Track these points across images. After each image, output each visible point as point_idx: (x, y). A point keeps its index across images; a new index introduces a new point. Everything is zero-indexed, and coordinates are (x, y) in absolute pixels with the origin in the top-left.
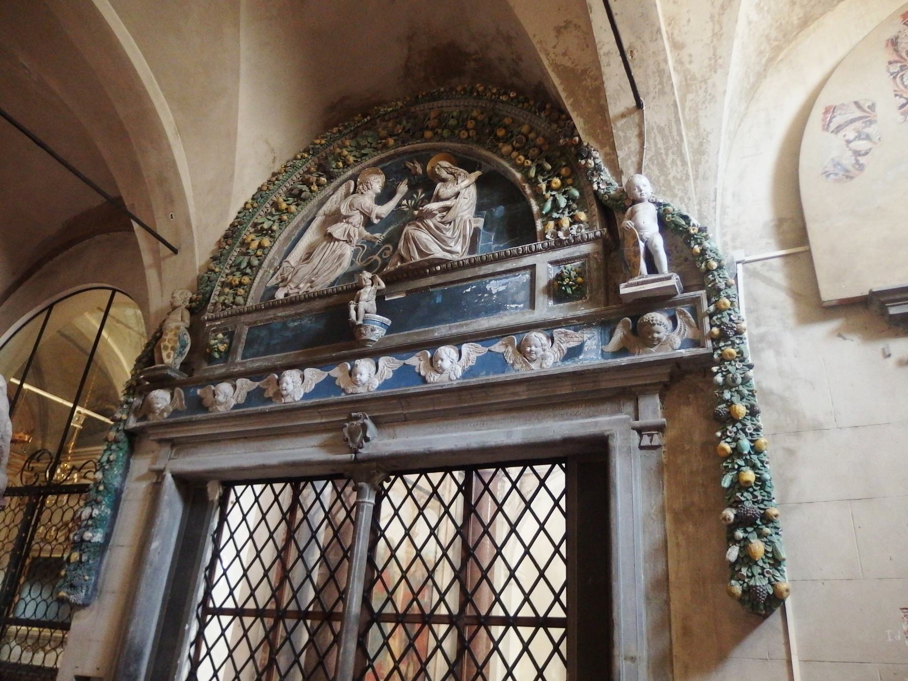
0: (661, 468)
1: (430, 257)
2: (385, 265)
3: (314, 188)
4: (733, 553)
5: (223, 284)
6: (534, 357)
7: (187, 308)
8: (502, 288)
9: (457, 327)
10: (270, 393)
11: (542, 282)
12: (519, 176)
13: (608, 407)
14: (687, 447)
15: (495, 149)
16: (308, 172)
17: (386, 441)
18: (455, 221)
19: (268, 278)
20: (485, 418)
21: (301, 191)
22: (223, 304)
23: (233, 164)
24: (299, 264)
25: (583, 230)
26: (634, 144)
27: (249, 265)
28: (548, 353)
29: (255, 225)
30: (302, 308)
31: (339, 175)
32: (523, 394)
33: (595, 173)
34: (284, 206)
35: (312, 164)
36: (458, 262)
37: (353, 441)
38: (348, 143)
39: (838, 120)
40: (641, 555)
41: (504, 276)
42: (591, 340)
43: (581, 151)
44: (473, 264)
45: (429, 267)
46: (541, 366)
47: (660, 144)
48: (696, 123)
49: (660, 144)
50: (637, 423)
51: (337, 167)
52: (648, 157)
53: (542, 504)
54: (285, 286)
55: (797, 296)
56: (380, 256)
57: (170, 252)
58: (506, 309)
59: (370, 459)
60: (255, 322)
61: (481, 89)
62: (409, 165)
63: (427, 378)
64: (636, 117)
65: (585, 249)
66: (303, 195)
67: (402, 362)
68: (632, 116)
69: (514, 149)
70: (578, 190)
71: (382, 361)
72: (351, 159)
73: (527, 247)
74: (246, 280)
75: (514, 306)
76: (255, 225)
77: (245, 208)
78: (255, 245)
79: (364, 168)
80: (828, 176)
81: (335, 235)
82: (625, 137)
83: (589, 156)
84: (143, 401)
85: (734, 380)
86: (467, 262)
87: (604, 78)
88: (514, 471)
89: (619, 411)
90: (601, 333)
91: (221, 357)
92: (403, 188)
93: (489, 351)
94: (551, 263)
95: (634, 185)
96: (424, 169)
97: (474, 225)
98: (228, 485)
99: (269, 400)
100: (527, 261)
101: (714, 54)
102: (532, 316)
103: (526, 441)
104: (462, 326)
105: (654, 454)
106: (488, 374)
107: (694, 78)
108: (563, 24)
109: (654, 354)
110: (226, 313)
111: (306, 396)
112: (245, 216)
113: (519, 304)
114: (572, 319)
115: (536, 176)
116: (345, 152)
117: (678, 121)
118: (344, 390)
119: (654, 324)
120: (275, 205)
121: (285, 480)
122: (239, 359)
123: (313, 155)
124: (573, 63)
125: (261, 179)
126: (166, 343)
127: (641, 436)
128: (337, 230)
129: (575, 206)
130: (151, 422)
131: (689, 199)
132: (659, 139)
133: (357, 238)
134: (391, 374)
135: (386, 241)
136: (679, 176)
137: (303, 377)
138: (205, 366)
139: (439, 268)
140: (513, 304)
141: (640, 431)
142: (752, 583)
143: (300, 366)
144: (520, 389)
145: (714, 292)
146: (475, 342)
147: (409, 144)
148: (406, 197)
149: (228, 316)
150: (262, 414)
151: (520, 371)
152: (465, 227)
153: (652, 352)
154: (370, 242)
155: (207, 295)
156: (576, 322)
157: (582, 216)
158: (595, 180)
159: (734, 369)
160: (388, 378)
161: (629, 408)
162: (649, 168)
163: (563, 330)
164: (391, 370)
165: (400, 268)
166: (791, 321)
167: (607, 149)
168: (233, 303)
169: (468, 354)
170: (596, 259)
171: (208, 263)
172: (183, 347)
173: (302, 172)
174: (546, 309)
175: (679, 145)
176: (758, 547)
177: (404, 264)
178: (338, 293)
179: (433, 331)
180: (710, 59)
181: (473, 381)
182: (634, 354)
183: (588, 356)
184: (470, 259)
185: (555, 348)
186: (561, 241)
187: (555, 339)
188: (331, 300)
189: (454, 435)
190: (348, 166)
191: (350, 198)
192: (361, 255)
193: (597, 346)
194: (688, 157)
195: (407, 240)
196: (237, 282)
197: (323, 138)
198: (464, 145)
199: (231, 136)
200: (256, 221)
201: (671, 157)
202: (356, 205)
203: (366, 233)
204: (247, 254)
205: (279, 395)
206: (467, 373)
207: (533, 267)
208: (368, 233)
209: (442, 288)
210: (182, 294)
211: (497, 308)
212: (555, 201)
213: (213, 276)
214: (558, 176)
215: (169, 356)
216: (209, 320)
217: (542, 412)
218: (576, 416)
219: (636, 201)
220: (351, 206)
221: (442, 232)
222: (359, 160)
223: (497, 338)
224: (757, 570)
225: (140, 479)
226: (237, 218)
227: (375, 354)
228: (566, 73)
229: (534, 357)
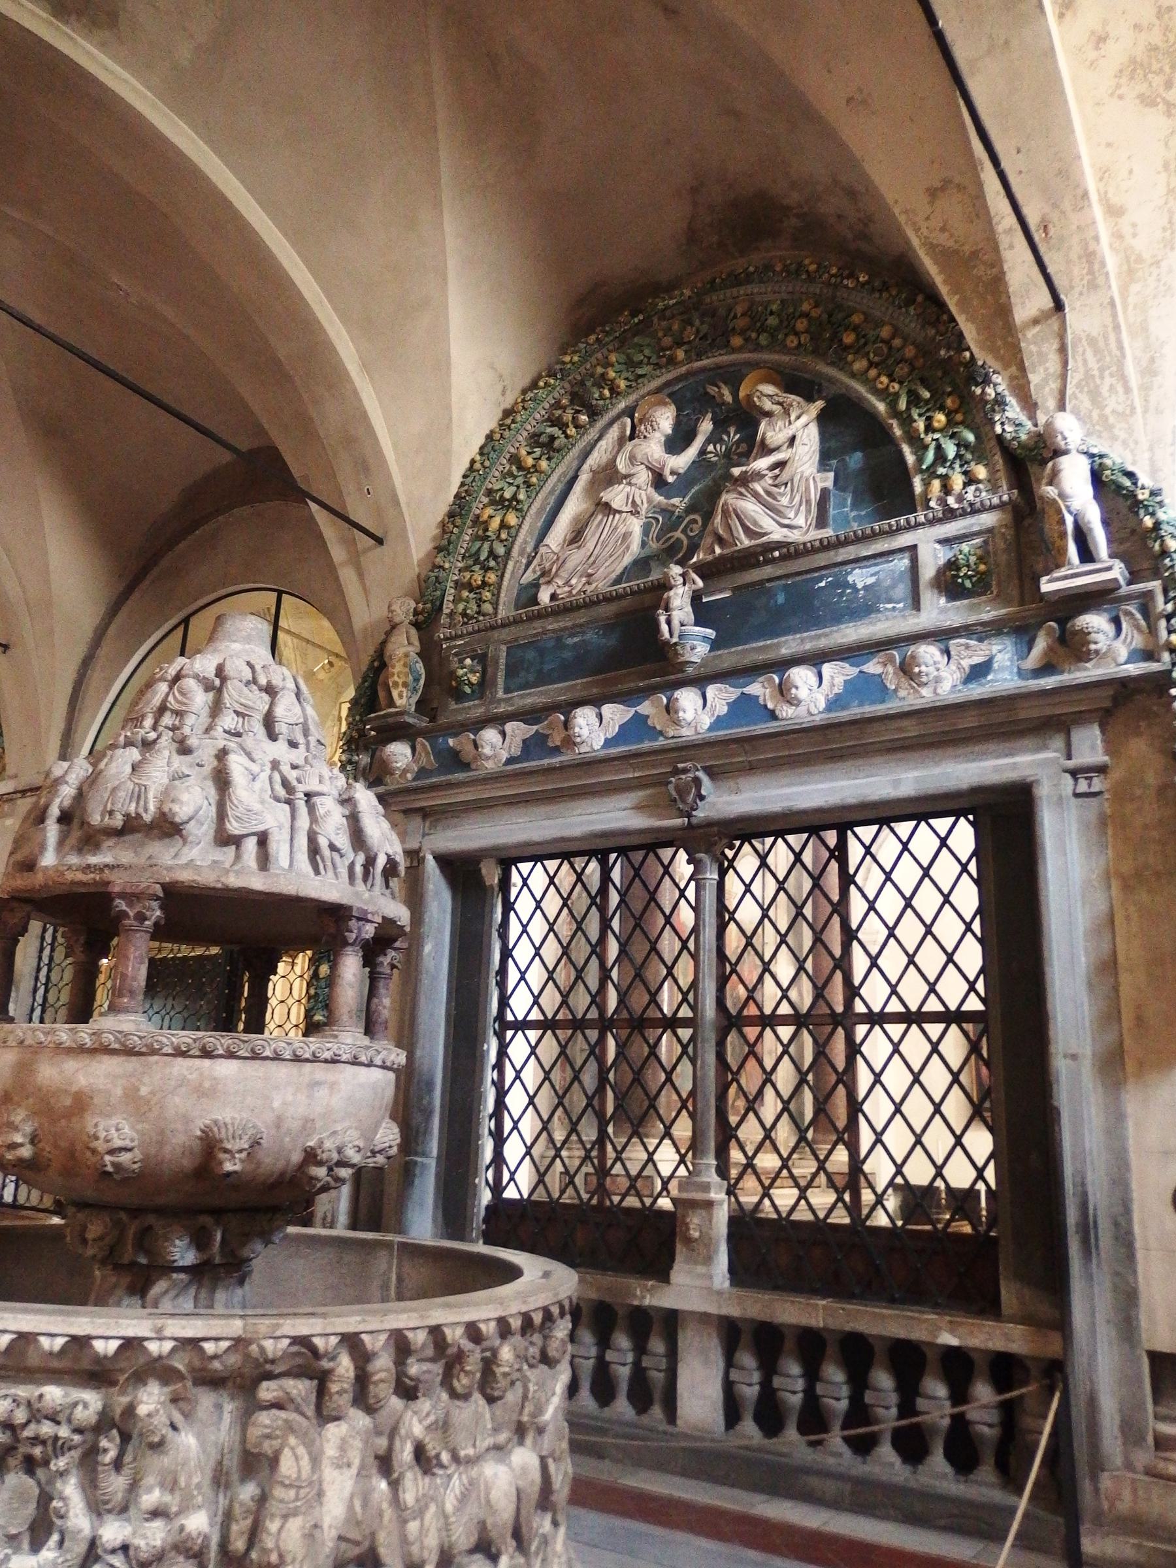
0: (1103, 821)
1: (764, 539)
2: (693, 549)
3: (572, 431)
5: (458, 585)
6: (924, 679)
7: (411, 623)
8: (871, 580)
9: (812, 638)
10: (556, 740)
11: (928, 572)
12: (881, 407)
13: (1027, 742)
14: (1138, 792)
15: (841, 363)
16: (557, 405)
17: (726, 798)
18: (792, 480)
19: (521, 572)
20: (860, 762)
21: (552, 438)
22: (464, 614)
23: (448, 407)
25: (984, 494)
26: (1053, 363)
27: (492, 554)
28: (943, 674)
29: (489, 492)
30: (581, 617)
32: (912, 729)
33: (996, 408)
34: (530, 461)
35: (559, 390)
36: (804, 544)
37: (684, 801)
38: (613, 358)
40: (1080, 931)
41: (872, 561)
42: (1002, 652)
43: (975, 375)
44: (826, 546)
45: (763, 553)
46: (935, 692)
48: (1144, 328)
50: (1071, 764)
51: (602, 397)
52: (1074, 382)
53: (945, 870)
54: (549, 583)
56: (684, 531)
58: (878, 611)
59: (709, 824)
60: (516, 640)
61: (813, 267)
62: (712, 390)
63: (777, 712)
64: (1054, 323)
65: (987, 520)
66: (556, 444)
67: (741, 690)
68: (1049, 322)
69: (871, 364)
70: (972, 430)
71: (711, 690)
72: (622, 384)
73: (902, 520)
74: (492, 577)
75: (890, 606)
77: (471, 468)
78: (495, 524)
79: (643, 397)
81: (615, 505)
82: (1040, 353)
83: (987, 381)
84: (372, 757)
86: (817, 544)
87: (1006, 267)
88: (904, 828)
89: (1045, 748)
90: (1016, 644)
91: (473, 691)
92: (706, 426)
93: (861, 672)
94: (940, 542)
95: (1055, 431)
96: (735, 394)
97: (821, 485)
98: (507, 860)
99: (556, 750)
101: (1170, 222)
102: (916, 620)
103: (922, 793)
104: (819, 637)
105: (1094, 802)
106: (861, 704)
107: (1140, 259)
108: (939, 185)
109: (1090, 672)
110: (470, 629)
111: (608, 743)
112: (473, 481)
113: (898, 603)
114: (974, 625)
115: (908, 409)
116: (612, 374)
117: (1117, 328)
118: (661, 733)
119: (1089, 633)
120: (515, 459)
121: (590, 854)
122: (500, 694)
123: (562, 379)
124: (956, 242)
125: (490, 423)
126: (396, 678)
127: (1076, 780)
128: (616, 496)
129: (969, 456)
130: (392, 787)
131: (1136, 443)
132: (1089, 354)
133: (646, 505)
134: (725, 709)
135: (690, 509)
136: (1120, 409)
137: (600, 717)
138: (453, 706)
139: (777, 554)
140: (889, 603)
141: (1074, 773)
143: (596, 702)
144: (905, 723)
146: (842, 660)
147: (708, 358)
148: (711, 439)
149: (474, 632)
150: (550, 770)
151: (907, 698)
152: (807, 489)
153: (1086, 669)
154: (665, 511)
155: (438, 603)
156: (980, 629)
157: (981, 472)
158: (997, 418)
160: (722, 714)
161: (1058, 742)
162: (1076, 398)
163: (962, 641)
164: (724, 702)
165: (721, 556)
167: (1013, 370)
168: (478, 613)
169: (832, 677)
170: (1003, 534)
171: (428, 555)
172: (417, 680)
173: (547, 406)
175: (1120, 364)
177: (726, 551)
178: (633, 593)
179: (778, 646)
180: (1164, 229)
181: (843, 715)
182: (1062, 672)
183: (1000, 676)
184: (821, 540)
185: (953, 667)
186: (952, 510)
187: (952, 653)
188: (624, 603)
189: (820, 786)
190: (618, 394)
191: (629, 446)
192: (655, 530)
193: (1011, 660)
194: (1134, 380)
195: (726, 513)
197: (574, 352)
198: (794, 358)
199: (442, 366)
200: (490, 486)
201: (1108, 381)
202: (639, 457)
203: (658, 498)
204: (485, 538)
205: (570, 742)
206: (834, 703)
207: (913, 548)
208: (661, 498)
209: (783, 582)
210: (403, 604)
211: (865, 608)
212: (939, 448)
213: (442, 574)
214: (942, 408)
215: (401, 696)
216: (446, 639)
217: (940, 752)
218: (984, 755)
219: (1058, 453)
220: (632, 459)
221: (775, 499)
222: (634, 384)
223: (872, 653)
226: (462, 484)
227: (700, 681)
228: (945, 256)
229: (924, 679)
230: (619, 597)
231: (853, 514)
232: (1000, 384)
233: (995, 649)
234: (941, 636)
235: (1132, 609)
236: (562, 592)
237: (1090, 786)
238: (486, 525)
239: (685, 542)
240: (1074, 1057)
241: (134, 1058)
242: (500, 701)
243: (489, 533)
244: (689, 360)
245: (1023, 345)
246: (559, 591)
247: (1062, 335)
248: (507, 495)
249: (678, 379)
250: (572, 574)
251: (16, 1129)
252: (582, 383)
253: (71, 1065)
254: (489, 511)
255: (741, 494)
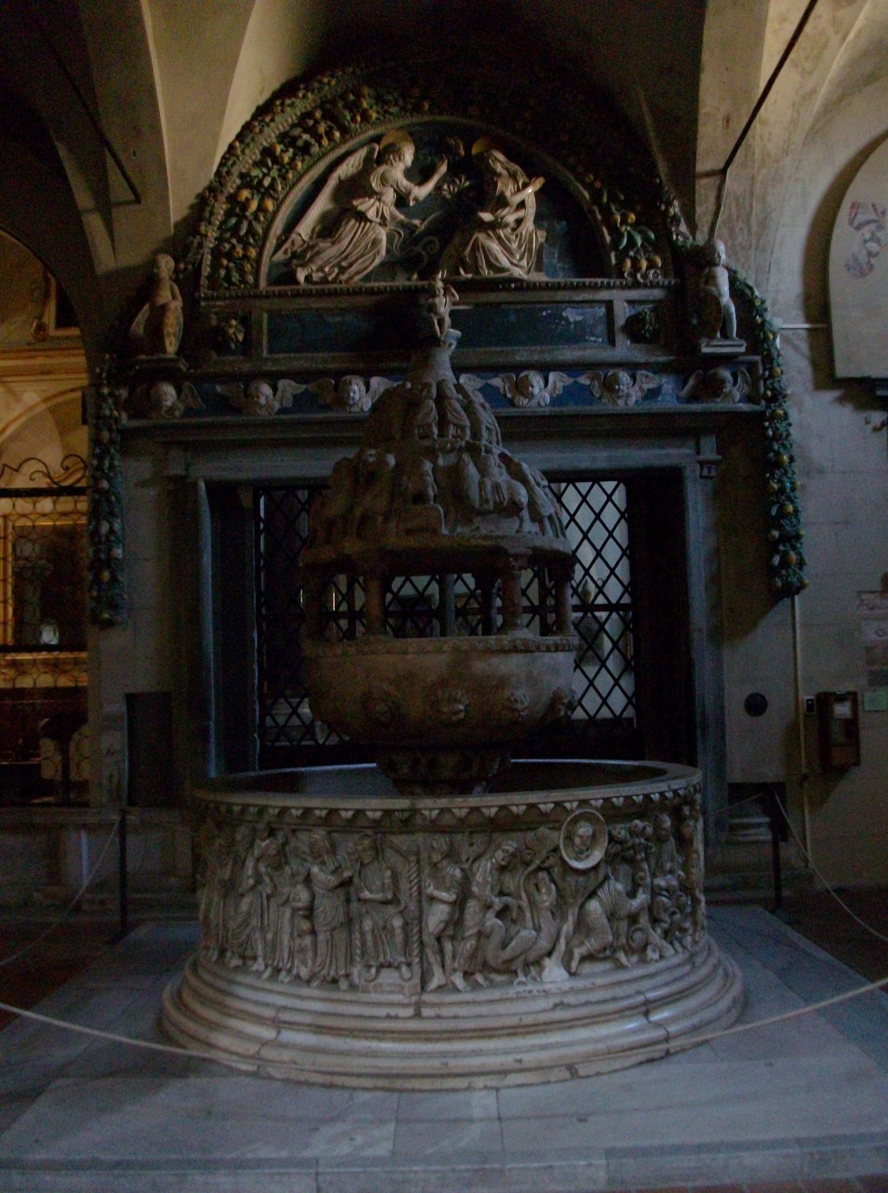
3: (325, 142)
4: (776, 560)
6: (621, 394)
8: (579, 318)
11: (620, 320)
16: (309, 115)
24: (311, 238)
26: (711, 204)
28: (632, 392)
29: (242, 176)
30: (344, 302)
31: (357, 134)
36: (534, 284)
38: (366, 91)
39: (861, 218)
42: (668, 384)
44: (547, 287)
46: (626, 404)
47: (734, 210)
48: (764, 199)
49: (734, 210)
50: (701, 457)
53: (611, 516)
55: (815, 365)
57: (132, 197)
58: (586, 341)
63: (516, 401)
67: (484, 382)
72: (374, 115)
75: (593, 339)
76: (242, 176)
78: (254, 205)
80: (849, 269)
83: (669, 204)
85: (781, 436)
87: (699, 136)
88: (584, 487)
92: (443, 169)
93: (576, 382)
96: (468, 148)
99: (327, 407)
100: (604, 295)
101: (789, 138)
105: (709, 481)
107: (769, 155)
109: (718, 405)
113: (598, 337)
117: (752, 193)
122: (265, 354)
128: (369, 207)
132: (733, 205)
135: (428, 232)
138: (214, 356)
139: (513, 285)
141: (702, 464)
142: (789, 580)
143: (366, 376)
145: (769, 359)
146: (561, 371)
148: (447, 178)
151: (605, 406)
157: (659, 262)
158: (673, 229)
159: (781, 426)
166: (810, 386)
169: (555, 383)
171: (185, 220)
173: (299, 113)
174: (625, 350)
176: (793, 556)
180: (785, 142)
184: (547, 283)
190: (368, 122)
193: (673, 390)
194: (754, 229)
196: (241, 255)
201: (740, 224)
202: (391, 181)
214: (633, 210)
215: (171, 344)
216: (206, 299)
224: (791, 572)
225: (142, 484)
226: (222, 165)
230: (371, 292)
231: (559, 265)
232: (675, 209)
233: (664, 380)
234: (632, 367)
235: (743, 369)
236: (316, 277)
237: (709, 472)
238: (245, 206)
239: (426, 258)
240: (700, 630)
241: (528, 654)
242: (267, 359)
243: (248, 214)
244: (431, 111)
245: (697, 187)
246: (314, 275)
247: (720, 189)
248: (267, 182)
249: (420, 124)
250: (328, 262)
251: (460, 702)
252: (333, 102)
253: (495, 660)
254: (245, 194)
255: (489, 235)
